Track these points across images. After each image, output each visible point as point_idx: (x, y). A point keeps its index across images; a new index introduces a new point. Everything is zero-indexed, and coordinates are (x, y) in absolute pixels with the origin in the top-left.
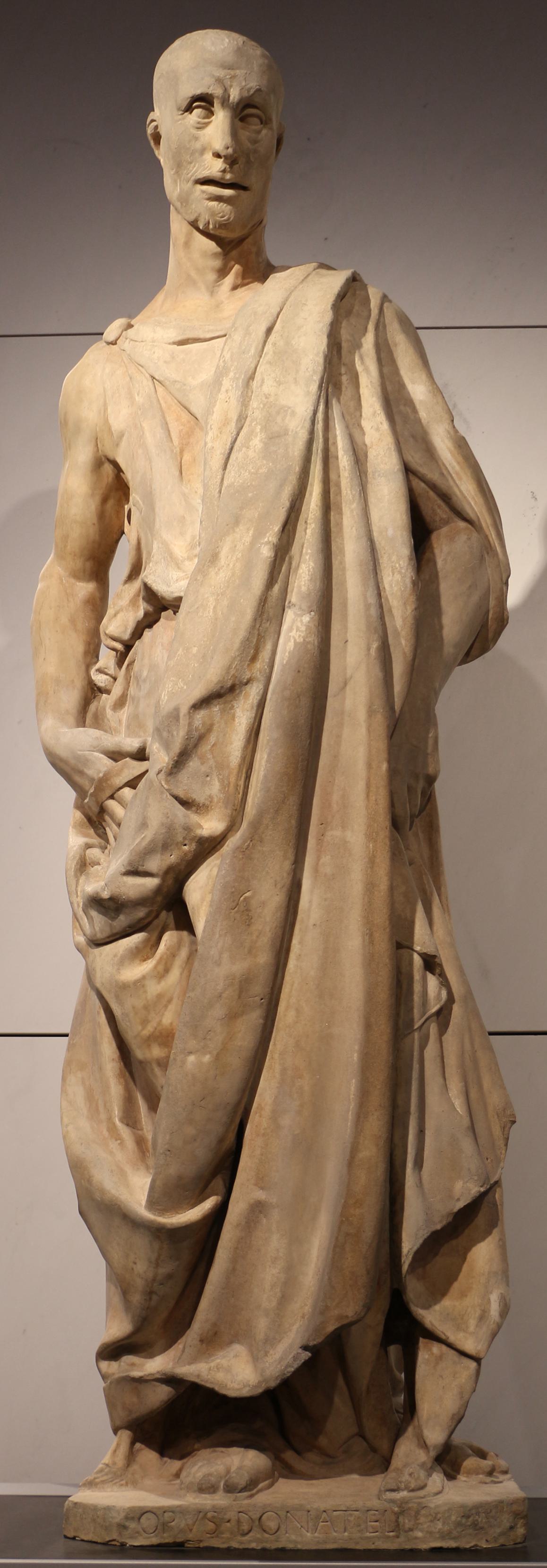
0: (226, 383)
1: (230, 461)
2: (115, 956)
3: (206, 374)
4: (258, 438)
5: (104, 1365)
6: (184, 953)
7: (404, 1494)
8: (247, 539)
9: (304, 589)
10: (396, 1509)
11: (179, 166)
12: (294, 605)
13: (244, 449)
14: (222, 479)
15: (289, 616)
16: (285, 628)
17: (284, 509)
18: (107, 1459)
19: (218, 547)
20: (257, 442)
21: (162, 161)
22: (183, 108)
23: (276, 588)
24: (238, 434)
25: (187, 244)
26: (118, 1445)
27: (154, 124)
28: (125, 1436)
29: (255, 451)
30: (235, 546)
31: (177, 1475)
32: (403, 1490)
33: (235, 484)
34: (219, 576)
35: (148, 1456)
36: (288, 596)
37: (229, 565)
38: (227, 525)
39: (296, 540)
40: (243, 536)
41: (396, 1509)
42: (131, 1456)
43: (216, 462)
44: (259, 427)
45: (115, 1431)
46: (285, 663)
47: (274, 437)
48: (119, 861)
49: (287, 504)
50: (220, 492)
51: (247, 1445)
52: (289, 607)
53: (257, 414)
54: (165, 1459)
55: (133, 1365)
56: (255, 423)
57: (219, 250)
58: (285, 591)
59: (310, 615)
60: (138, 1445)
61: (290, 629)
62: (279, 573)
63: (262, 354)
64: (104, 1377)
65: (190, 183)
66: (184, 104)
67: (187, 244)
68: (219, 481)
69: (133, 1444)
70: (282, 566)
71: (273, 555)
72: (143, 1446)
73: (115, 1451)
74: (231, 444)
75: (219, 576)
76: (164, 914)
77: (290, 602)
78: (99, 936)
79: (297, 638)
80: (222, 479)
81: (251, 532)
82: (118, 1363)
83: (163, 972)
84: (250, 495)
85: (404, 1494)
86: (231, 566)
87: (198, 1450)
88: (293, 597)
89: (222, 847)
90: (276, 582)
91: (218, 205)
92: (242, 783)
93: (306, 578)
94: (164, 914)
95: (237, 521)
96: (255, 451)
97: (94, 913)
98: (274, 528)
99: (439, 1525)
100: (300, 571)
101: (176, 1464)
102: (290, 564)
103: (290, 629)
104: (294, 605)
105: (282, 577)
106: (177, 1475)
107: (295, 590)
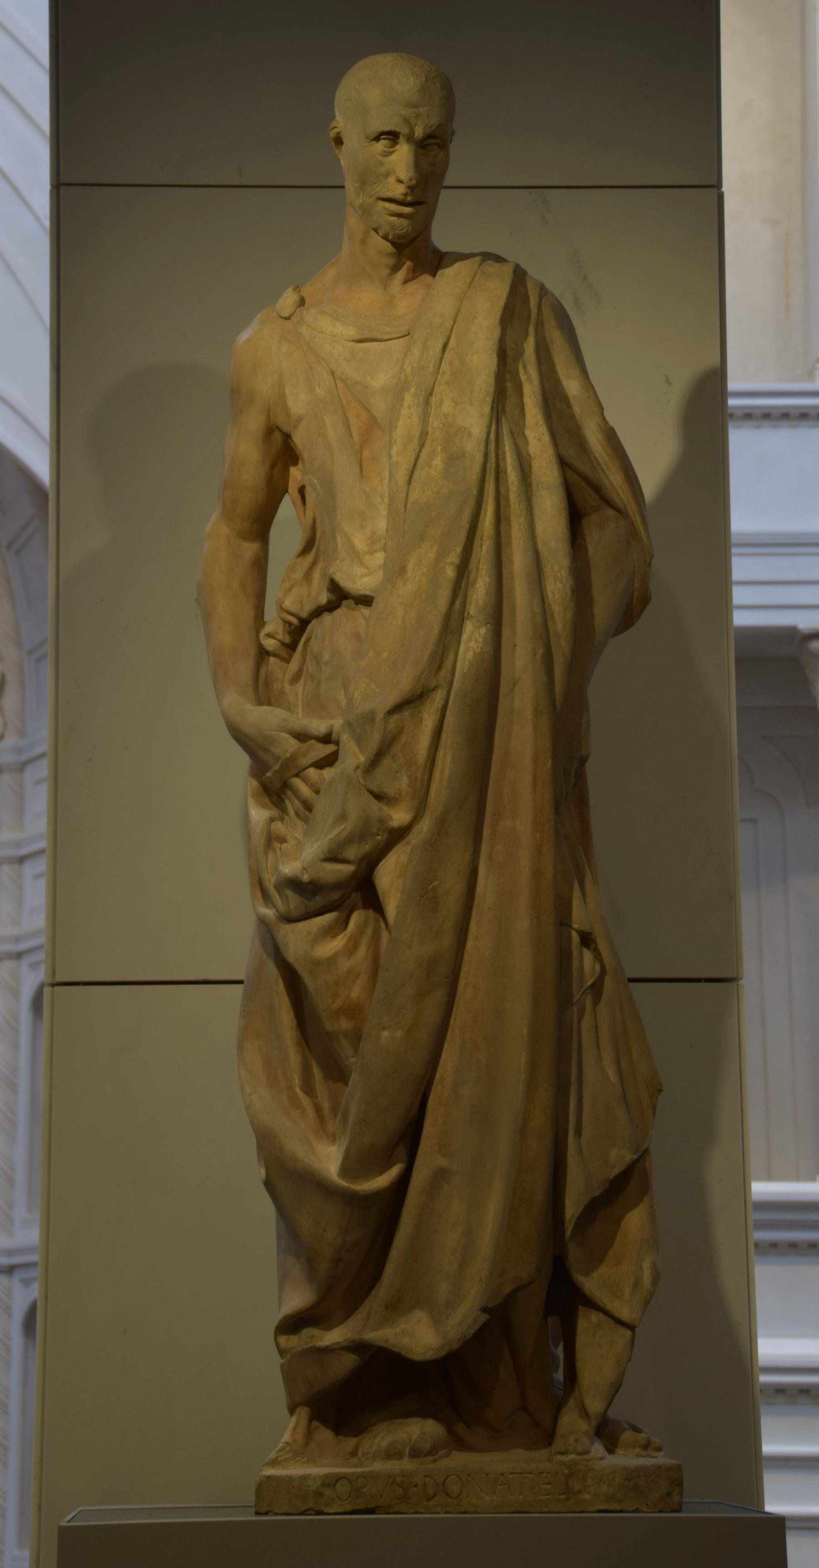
0: (408, 399)
1: (415, 477)
2: (309, 933)
3: (381, 380)
4: (439, 458)
5: (283, 1339)
6: (369, 931)
7: (572, 1457)
8: (432, 554)
9: (481, 602)
10: (566, 1471)
11: (363, 183)
12: (472, 617)
13: (427, 468)
14: (407, 494)
15: (469, 627)
16: (465, 637)
17: (465, 531)
18: (286, 1437)
19: (405, 561)
20: (438, 462)
21: (342, 161)
22: (372, 138)
23: (458, 603)
24: (420, 451)
25: (364, 241)
26: (297, 1423)
27: (336, 130)
28: (303, 1413)
29: (436, 470)
30: (421, 560)
31: (354, 1453)
32: (571, 1453)
33: (420, 501)
34: (407, 588)
35: (325, 1434)
36: (467, 608)
37: (415, 577)
38: (414, 541)
39: (473, 556)
40: (428, 552)
41: (566, 1471)
42: (309, 1434)
43: (401, 477)
44: (439, 449)
45: (292, 1412)
46: (465, 671)
47: (453, 459)
48: (315, 846)
49: (467, 526)
50: (406, 506)
51: (424, 1414)
52: (468, 619)
53: (438, 434)
54: (340, 1437)
55: (313, 1337)
56: (436, 443)
57: (394, 250)
58: (464, 605)
59: (487, 626)
60: (315, 1423)
61: (469, 640)
62: (460, 589)
63: (439, 370)
64: (282, 1352)
65: (372, 199)
66: (374, 135)
67: (364, 241)
68: (405, 495)
69: (310, 1421)
70: (462, 581)
71: (456, 574)
72: (319, 1425)
73: (295, 1429)
74: (415, 460)
75: (407, 588)
76: (354, 894)
77: (468, 614)
78: (294, 914)
79: (475, 648)
80: (407, 494)
81: (435, 550)
82: (297, 1336)
83: (351, 948)
84: (433, 514)
85: (572, 1457)
86: (417, 579)
87: (374, 1425)
88: (472, 610)
89: (407, 835)
90: (458, 597)
91: (398, 220)
92: (426, 778)
93: (483, 593)
94: (354, 894)
95: (422, 538)
96: (436, 470)
97: (289, 893)
98: (457, 550)
99: (605, 1488)
100: (478, 585)
101: (352, 1442)
102: (468, 577)
103: (469, 640)
104: (472, 617)
105: (462, 590)
106: (354, 1453)
107: (473, 603)
